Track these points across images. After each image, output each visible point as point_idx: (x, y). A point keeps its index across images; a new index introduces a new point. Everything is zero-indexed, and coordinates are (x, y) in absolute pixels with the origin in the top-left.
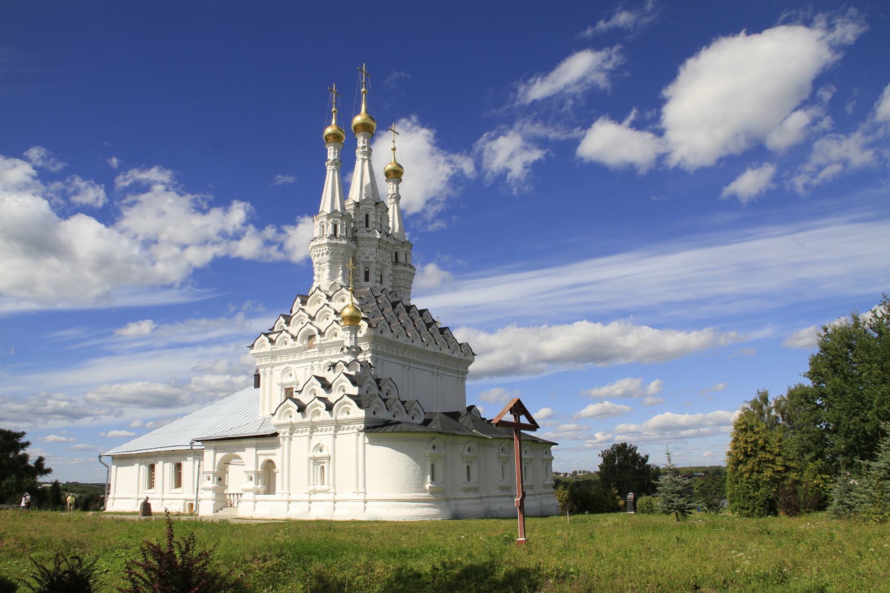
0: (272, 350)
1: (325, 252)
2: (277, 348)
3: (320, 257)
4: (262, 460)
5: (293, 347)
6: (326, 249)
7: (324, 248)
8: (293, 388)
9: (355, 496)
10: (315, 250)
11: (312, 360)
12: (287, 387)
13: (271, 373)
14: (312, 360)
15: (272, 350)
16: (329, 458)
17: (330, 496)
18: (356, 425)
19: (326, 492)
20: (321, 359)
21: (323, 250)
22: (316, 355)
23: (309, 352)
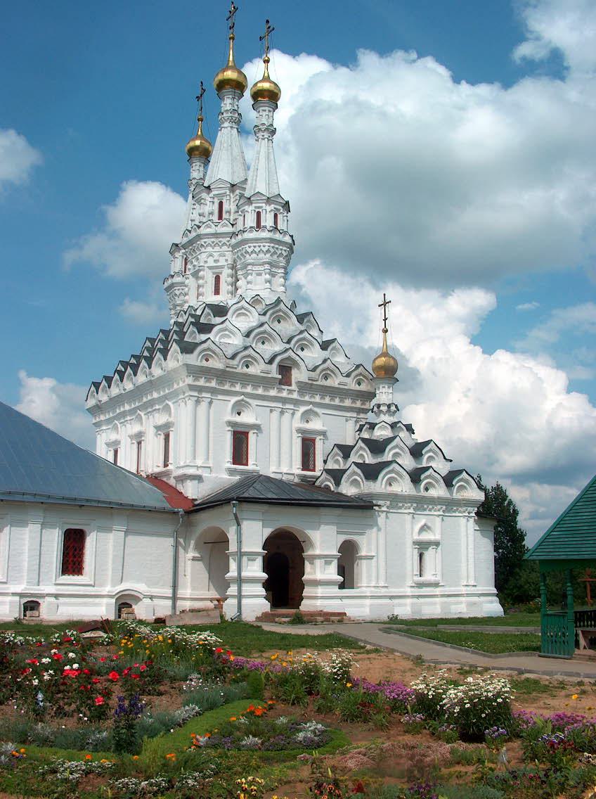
0: (228, 369)
1: (285, 254)
2: (236, 368)
3: (275, 257)
4: (343, 538)
5: (262, 374)
6: (285, 251)
7: (285, 248)
8: (248, 433)
9: (471, 590)
10: (272, 245)
11: (284, 401)
12: (239, 429)
13: (210, 403)
14: (284, 401)
15: (228, 369)
16: (437, 544)
17: (438, 591)
18: (469, 509)
19: (436, 585)
20: (296, 403)
21: (281, 249)
22: (290, 396)
23: (284, 390)
